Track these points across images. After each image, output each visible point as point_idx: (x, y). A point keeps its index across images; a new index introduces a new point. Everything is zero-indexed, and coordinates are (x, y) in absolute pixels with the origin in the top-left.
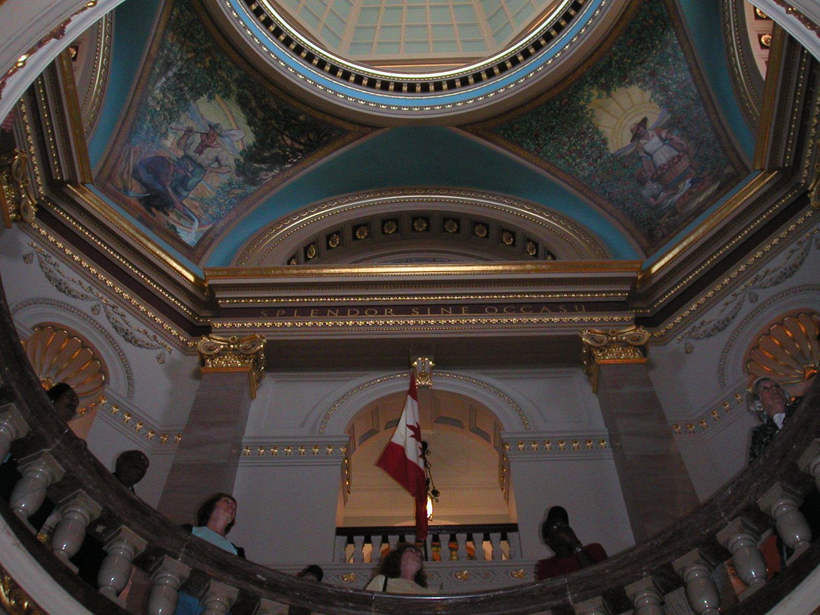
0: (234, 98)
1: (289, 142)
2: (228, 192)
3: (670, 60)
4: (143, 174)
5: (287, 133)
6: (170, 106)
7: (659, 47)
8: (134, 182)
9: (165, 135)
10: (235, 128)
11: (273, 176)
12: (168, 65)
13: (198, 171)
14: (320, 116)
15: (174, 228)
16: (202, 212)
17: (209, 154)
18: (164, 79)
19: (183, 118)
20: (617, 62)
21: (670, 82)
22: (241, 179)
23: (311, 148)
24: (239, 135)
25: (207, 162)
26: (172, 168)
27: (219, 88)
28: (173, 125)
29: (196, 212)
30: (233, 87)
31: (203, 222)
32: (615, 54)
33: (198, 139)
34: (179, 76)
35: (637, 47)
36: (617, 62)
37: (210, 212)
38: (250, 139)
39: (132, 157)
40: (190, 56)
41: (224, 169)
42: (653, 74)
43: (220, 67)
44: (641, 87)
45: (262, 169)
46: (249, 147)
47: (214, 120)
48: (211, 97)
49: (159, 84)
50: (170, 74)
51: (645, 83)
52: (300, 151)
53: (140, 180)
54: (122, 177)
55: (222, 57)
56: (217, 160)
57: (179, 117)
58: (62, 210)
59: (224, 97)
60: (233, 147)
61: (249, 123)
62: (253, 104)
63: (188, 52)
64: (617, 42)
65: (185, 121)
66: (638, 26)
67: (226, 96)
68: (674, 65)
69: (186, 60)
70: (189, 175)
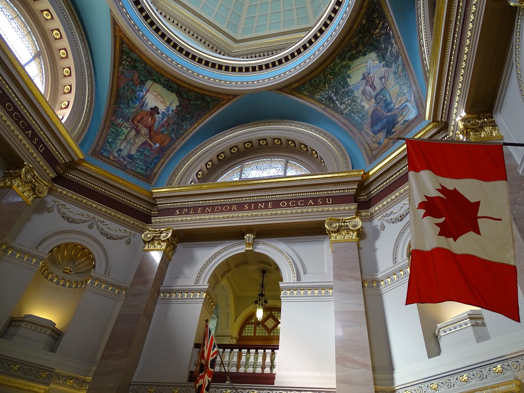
0: (350, 63)
1: (377, 31)
2: (399, 76)
4: (377, 128)
5: (372, 32)
6: (350, 101)
8: (378, 136)
9: (363, 107)
10: (366, 64)
11: (396, 44)
12: (330, 99)
13: (383, 92)
14: (363, 11)
15: (406, 121)
16: (404, 97)
17: (377, 83)
18: (337, 102)
19: (356, 94)
22: (393, 65)
23: (383, 17)
24: (370, 62)
25: (381, 85)
26: (379, 108)
27: (345, 71)
28: (359, 101)
29: (403, 102)
30: (344, 63)
31: (409, 99)
33: (368, 88)
34: (336, 93)
37: (406, 91)
38: (373, 55)
39: (368, 131)
40: (327, 86)
41: (387, 75)
43: (333, 70)
45: (391, 50)
46: (378, 56)
47: (361, 77)
48: (349, 76)
49: (339, 105)
50: (334, 98)
52: (384, 24)
53: (379, 131)
54: (374, 142)
55: (328, 69)
56: (381, 79)
57: (355, 97)
58: (373, 190)
59: (349, 69)
60: (377, 66)
61: (365, 55)
62: (354, 52)
63: (325, 87)
65: (358, 94)
67: (349, 67)
69: (329, 88)
70: (385, 98)
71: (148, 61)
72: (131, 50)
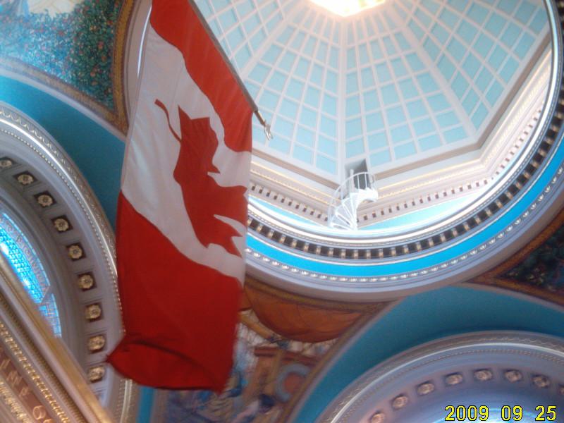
3: (54, 56)
7: (71, 59)
20: (102, 21)
21: (40, 40)
32: (108, 26)
35: (92, 45)
36: (102, 21)
42: (60, 33)
44: (64, 15)
51: (62, 21)
64: (112, 38)
66: (104, 64)
68: (47, 55)
71: (541, 239)
72: (520, 264)
